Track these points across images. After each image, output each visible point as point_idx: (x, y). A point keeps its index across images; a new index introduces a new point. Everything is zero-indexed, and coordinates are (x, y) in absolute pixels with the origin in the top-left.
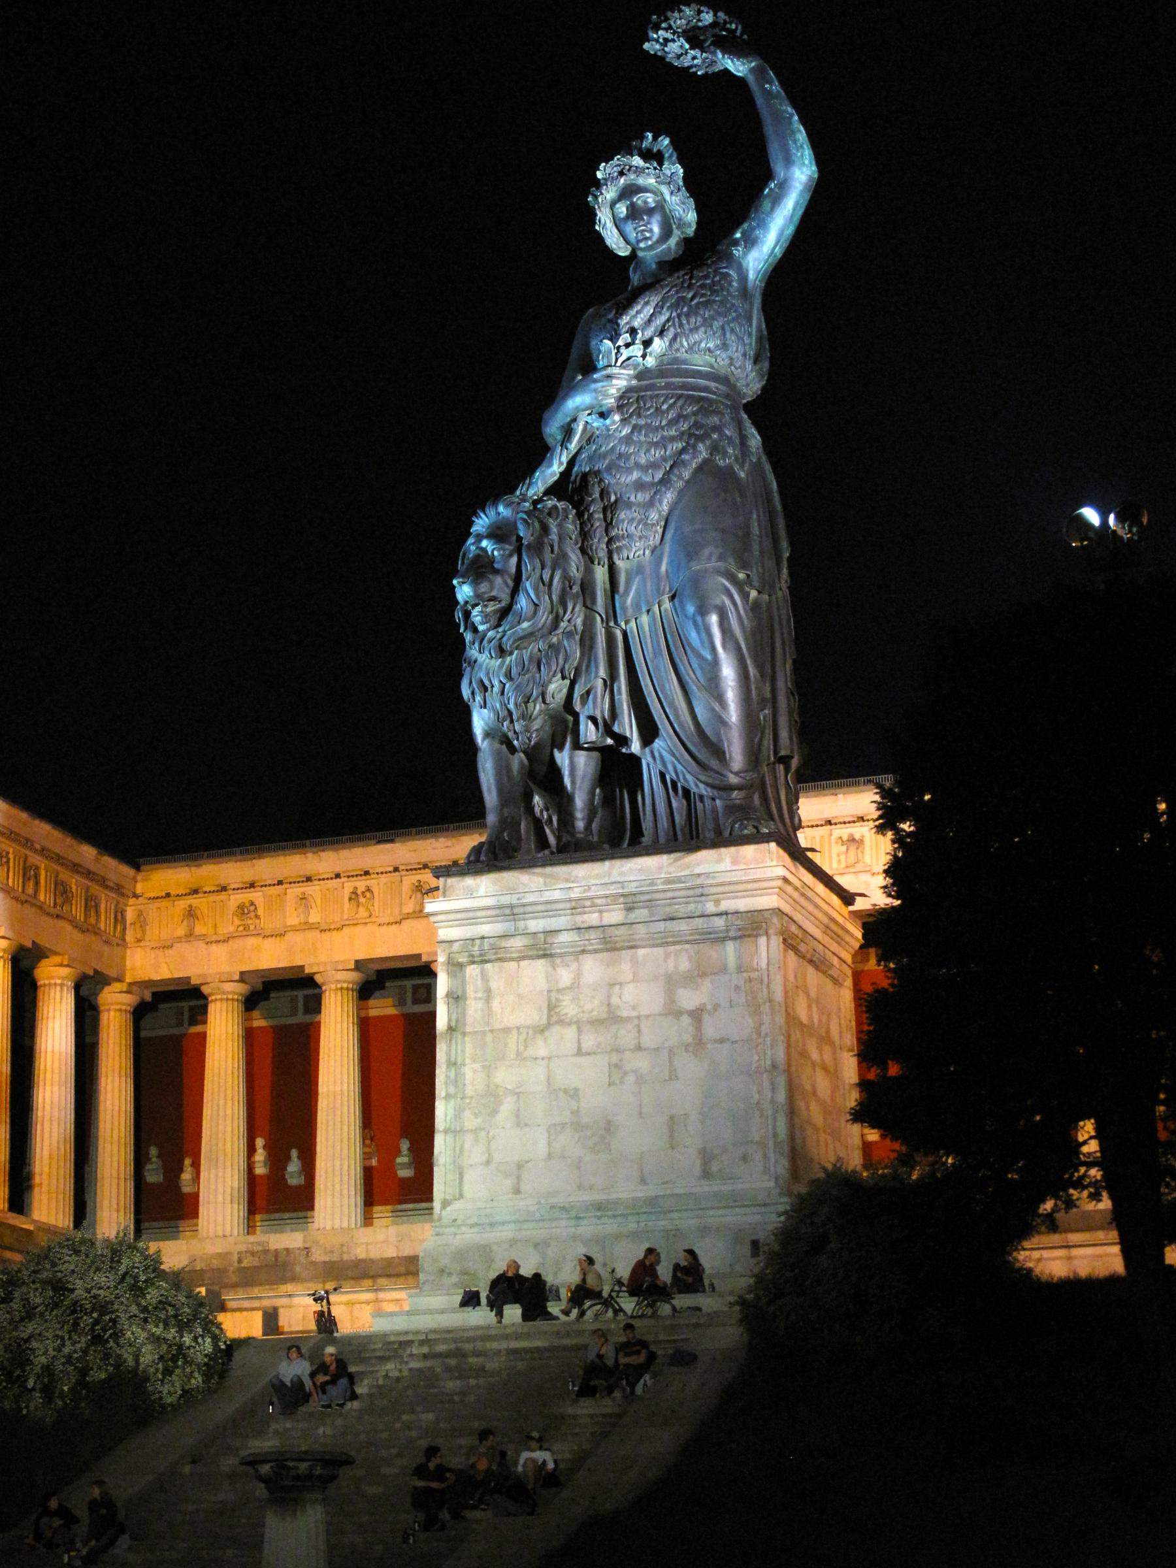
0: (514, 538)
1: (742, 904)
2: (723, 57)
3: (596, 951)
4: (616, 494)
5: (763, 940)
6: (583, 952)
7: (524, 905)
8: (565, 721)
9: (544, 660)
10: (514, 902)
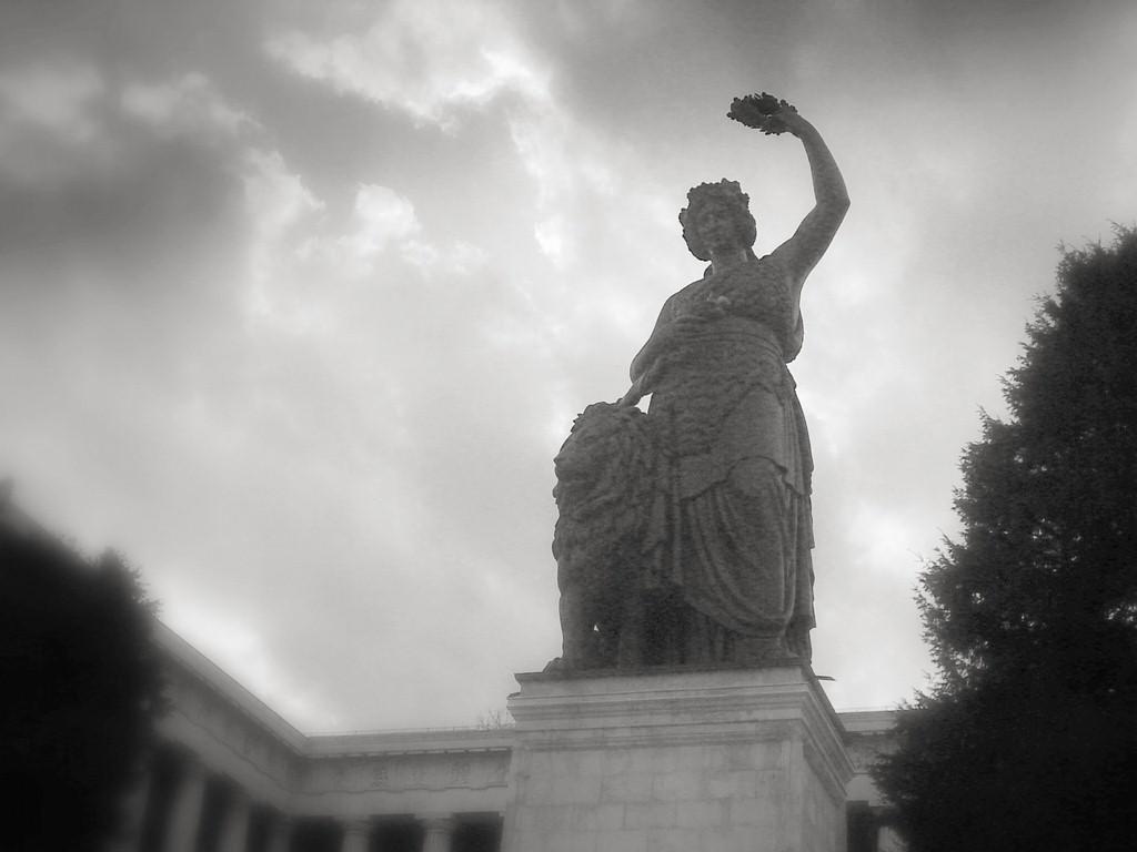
1: (771, 715)
3: (644, 746)
5: (786, 746)
6: (635, 746)
7: (588, 705)
10: (581, 702)
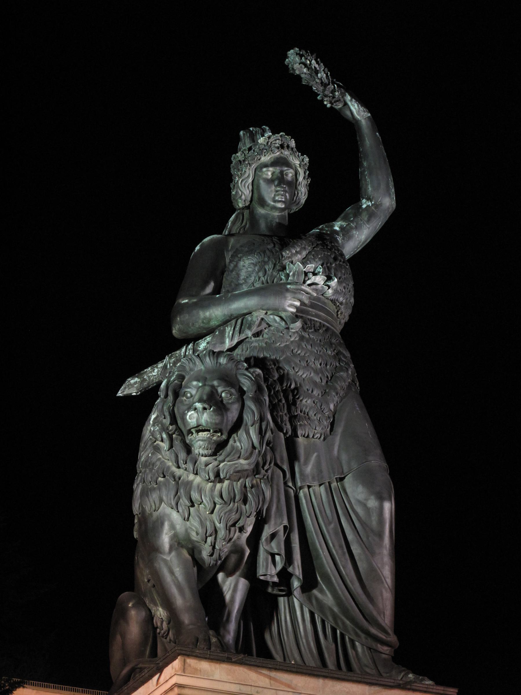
0: (238, 387)
2: (351, 100)
4: (296, 384)
8: (242, 553)
9: (249, 495)
